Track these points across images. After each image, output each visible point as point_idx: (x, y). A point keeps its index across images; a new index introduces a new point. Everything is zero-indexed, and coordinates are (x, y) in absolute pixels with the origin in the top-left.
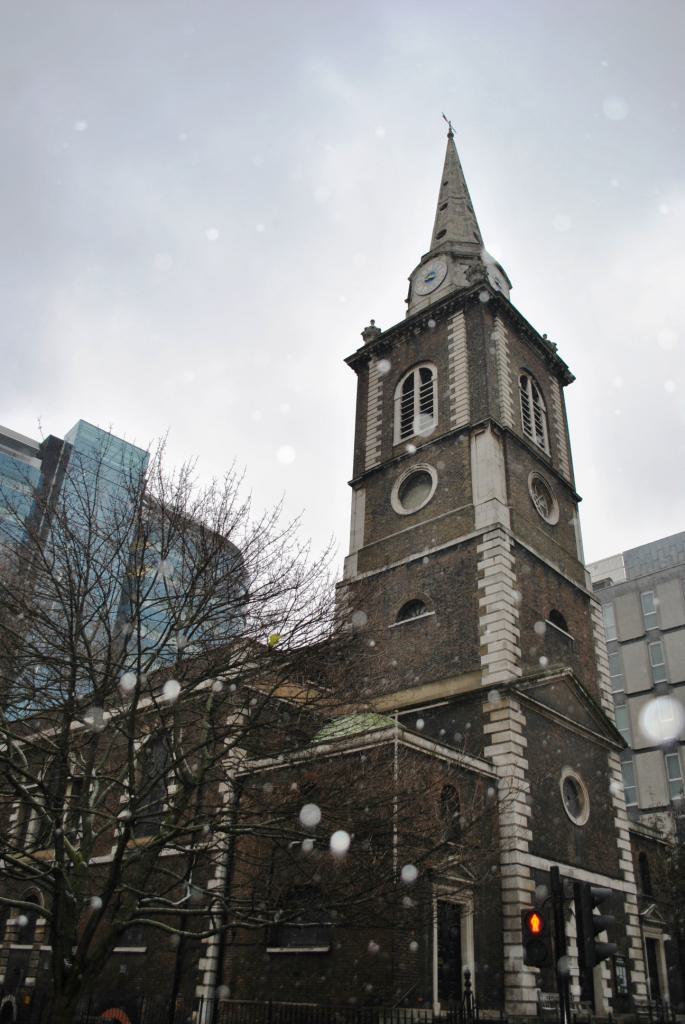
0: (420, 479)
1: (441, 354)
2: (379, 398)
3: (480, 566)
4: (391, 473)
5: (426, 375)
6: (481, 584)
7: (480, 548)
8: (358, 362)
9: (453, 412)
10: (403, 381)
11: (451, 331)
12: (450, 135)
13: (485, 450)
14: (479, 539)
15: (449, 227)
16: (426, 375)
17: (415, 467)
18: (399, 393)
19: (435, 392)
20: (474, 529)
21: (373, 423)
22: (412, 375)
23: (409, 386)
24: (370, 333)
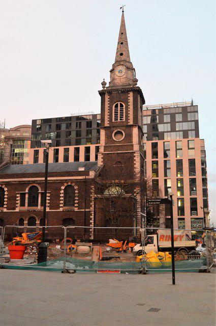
0: (120, 133)
1: (126, 101)
2: (108, 107)
3: (135, 158)
4: (112, 129)
5: (121, 106)
6: (135, 162)
7: (135, 155)
8: (102, 94)
9: (129, 119)
10: (114, 105)
11: (129, 97)
12: (123, 12)
13: (135, 131)
14: (135, 153)
15: (124, 53)
16: (121, 106)
17: (119, 130)
18: (114, 108)
19: (124, 111)
20: (133, 150)
21: (107, 113)
22: (117, 104)
23: (116, 106)
24: (104, 84)
